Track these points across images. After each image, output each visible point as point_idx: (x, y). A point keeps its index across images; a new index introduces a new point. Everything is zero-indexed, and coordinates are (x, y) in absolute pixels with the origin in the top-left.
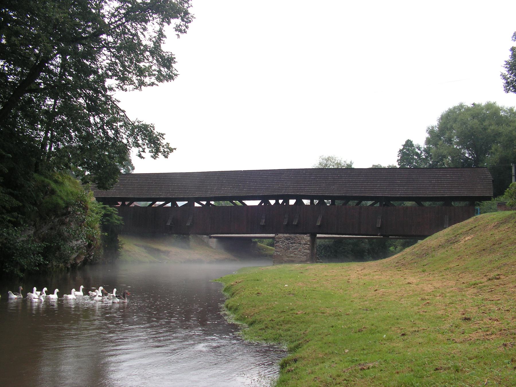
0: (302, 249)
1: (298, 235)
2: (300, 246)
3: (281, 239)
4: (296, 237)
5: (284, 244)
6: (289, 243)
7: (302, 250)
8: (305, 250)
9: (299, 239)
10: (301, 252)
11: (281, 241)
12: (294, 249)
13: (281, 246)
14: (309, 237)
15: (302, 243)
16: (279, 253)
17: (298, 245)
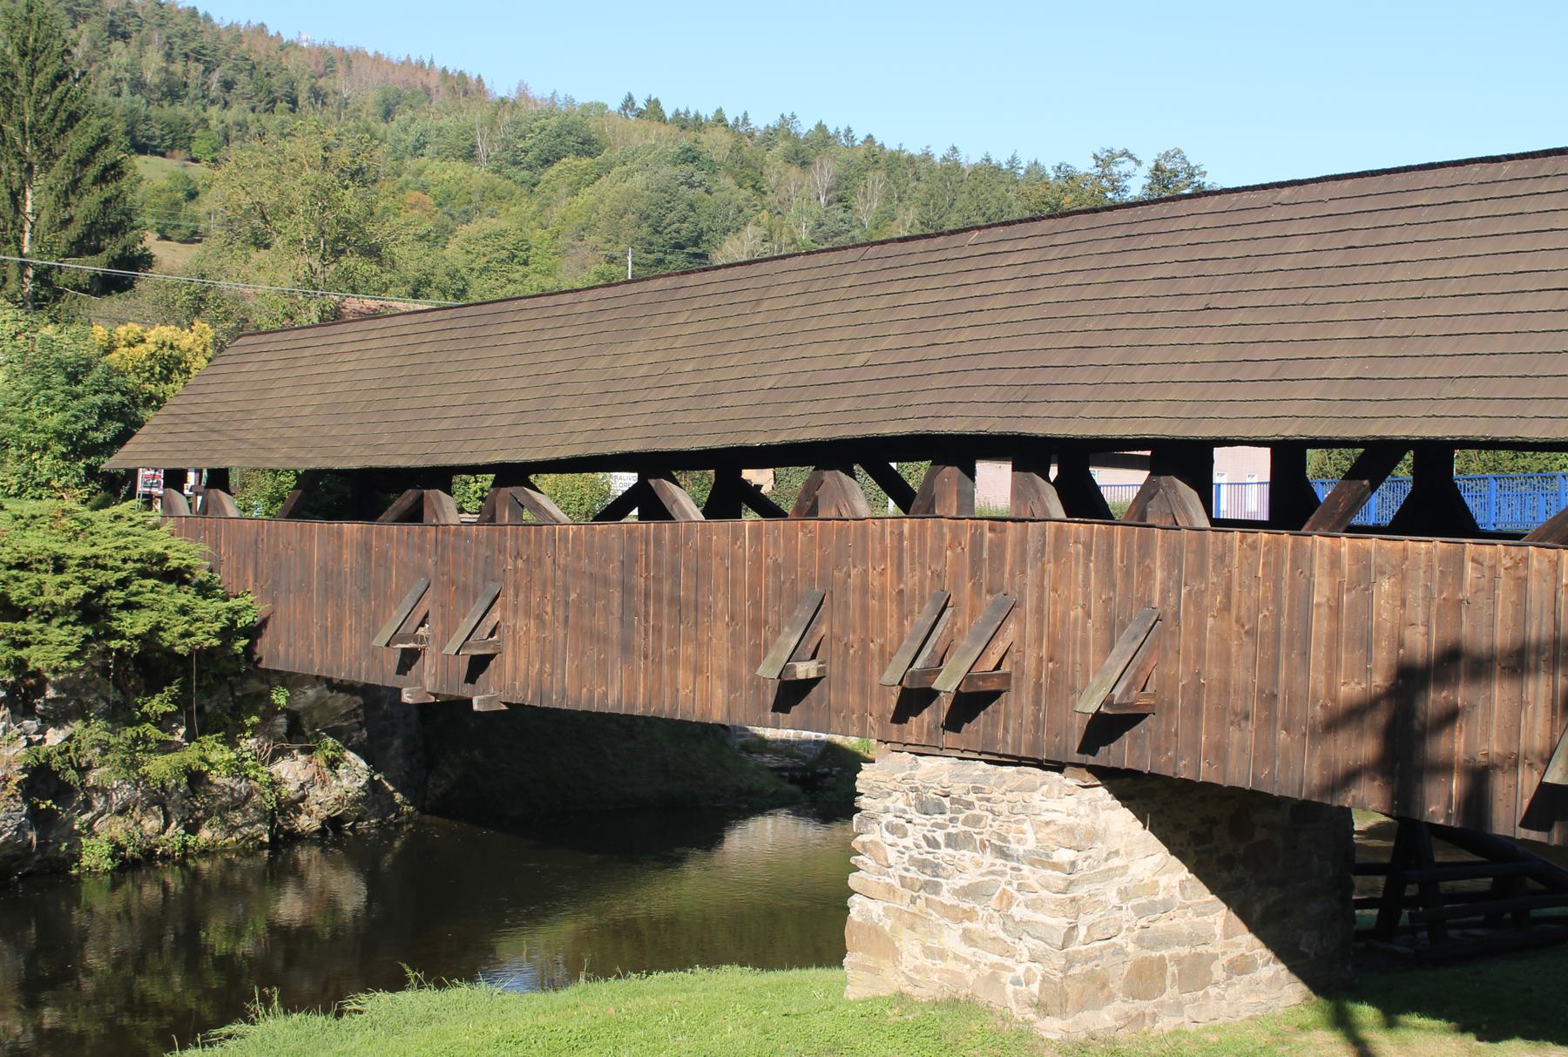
2: (1003, 874)
3: (888, 802)
6: (940, 836)
7: (1014, 910)
8: (1039, 917)
12: (967, 892)
13: (892, 855)
17: (988, 858)
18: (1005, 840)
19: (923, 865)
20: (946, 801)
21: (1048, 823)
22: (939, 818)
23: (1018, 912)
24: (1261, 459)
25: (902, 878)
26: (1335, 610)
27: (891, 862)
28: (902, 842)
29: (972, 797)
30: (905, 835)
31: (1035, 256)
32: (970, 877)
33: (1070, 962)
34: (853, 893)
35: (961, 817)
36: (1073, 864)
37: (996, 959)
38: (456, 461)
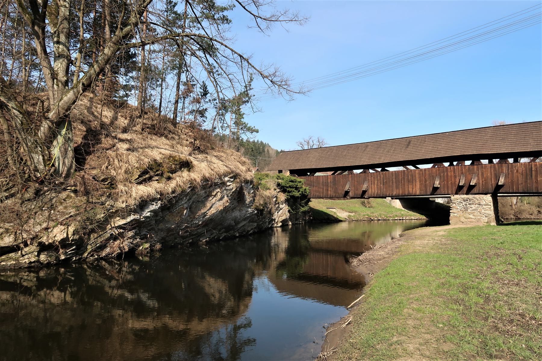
6: (467, 204)
7: (482, 211)
10: (481, 213)
12: (473, 210)
13: (458, 207)
15: (481, 204)
17: (477, 205)
23: (483, 211)
28: (460, 206)
31: (463, 135)
32: (474, 208)
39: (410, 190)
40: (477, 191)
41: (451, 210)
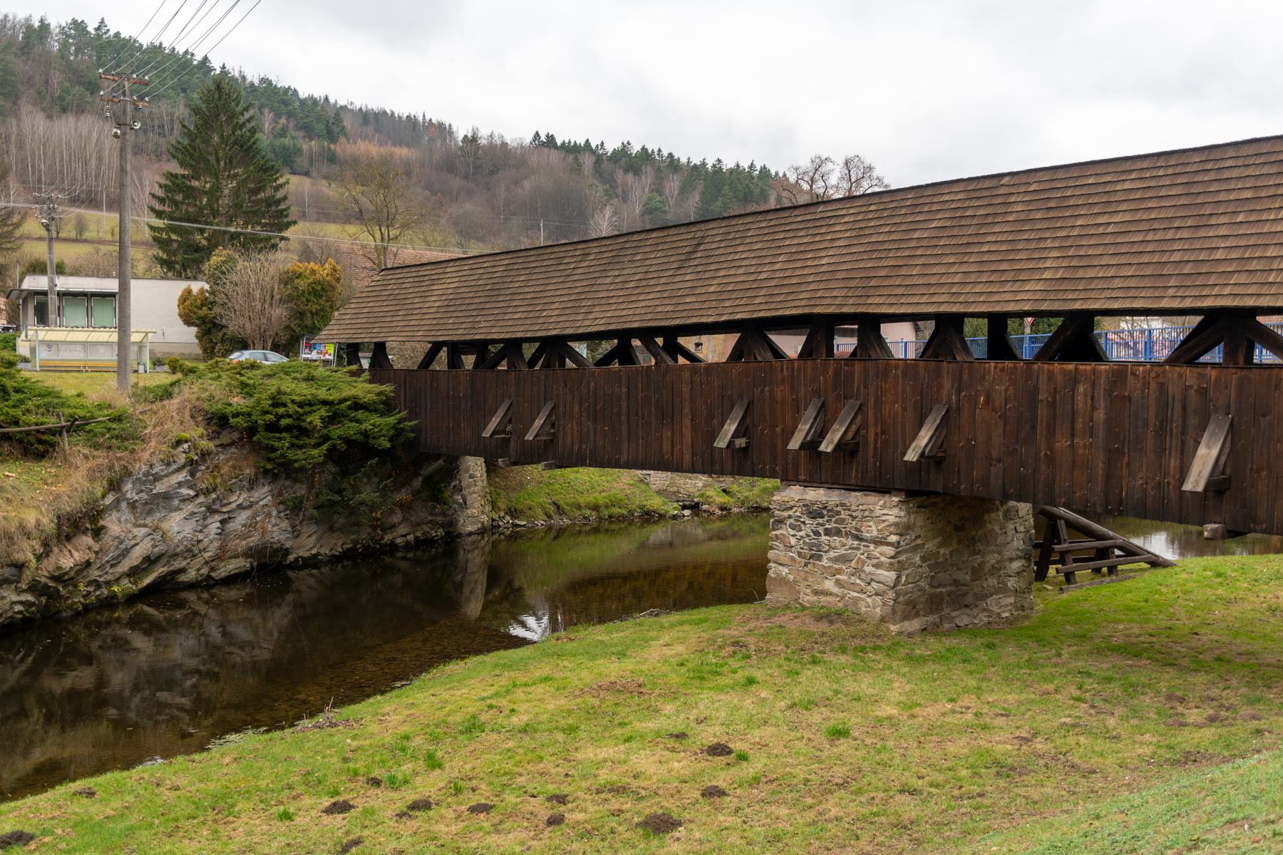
0: (864, 563)
1: (855, 498)
2: (858, 549)
3: (791, 512)
4: (842, 505)
5: (802, 533)
6: (821, 530)
8: (879, 572)
9: (854, 518)
10: (863, 576)
11: (790, 517)
12: (836, 560)
13: (793, 541)
14: (896, 511)
15: (866, 535)
16: (785, 571)
17: (850, 542)
18: (859, 530)
19: (811, 547)
20: (825, 512)
21: (884, 521)
22: (820, 521)
24: (984, 323)
25: (799, 553)
26: (1053, 405)
27: (793, 544)
29: (839, 509)
30: (800, 530)
33: (898, 595)
34: (770, 561)
35: (834, 519)
36: (899, 542)
37: (856, 594)
38: (1097, 306)
39: (666, 447)
40: (856, 477)
41: (772, 548)
